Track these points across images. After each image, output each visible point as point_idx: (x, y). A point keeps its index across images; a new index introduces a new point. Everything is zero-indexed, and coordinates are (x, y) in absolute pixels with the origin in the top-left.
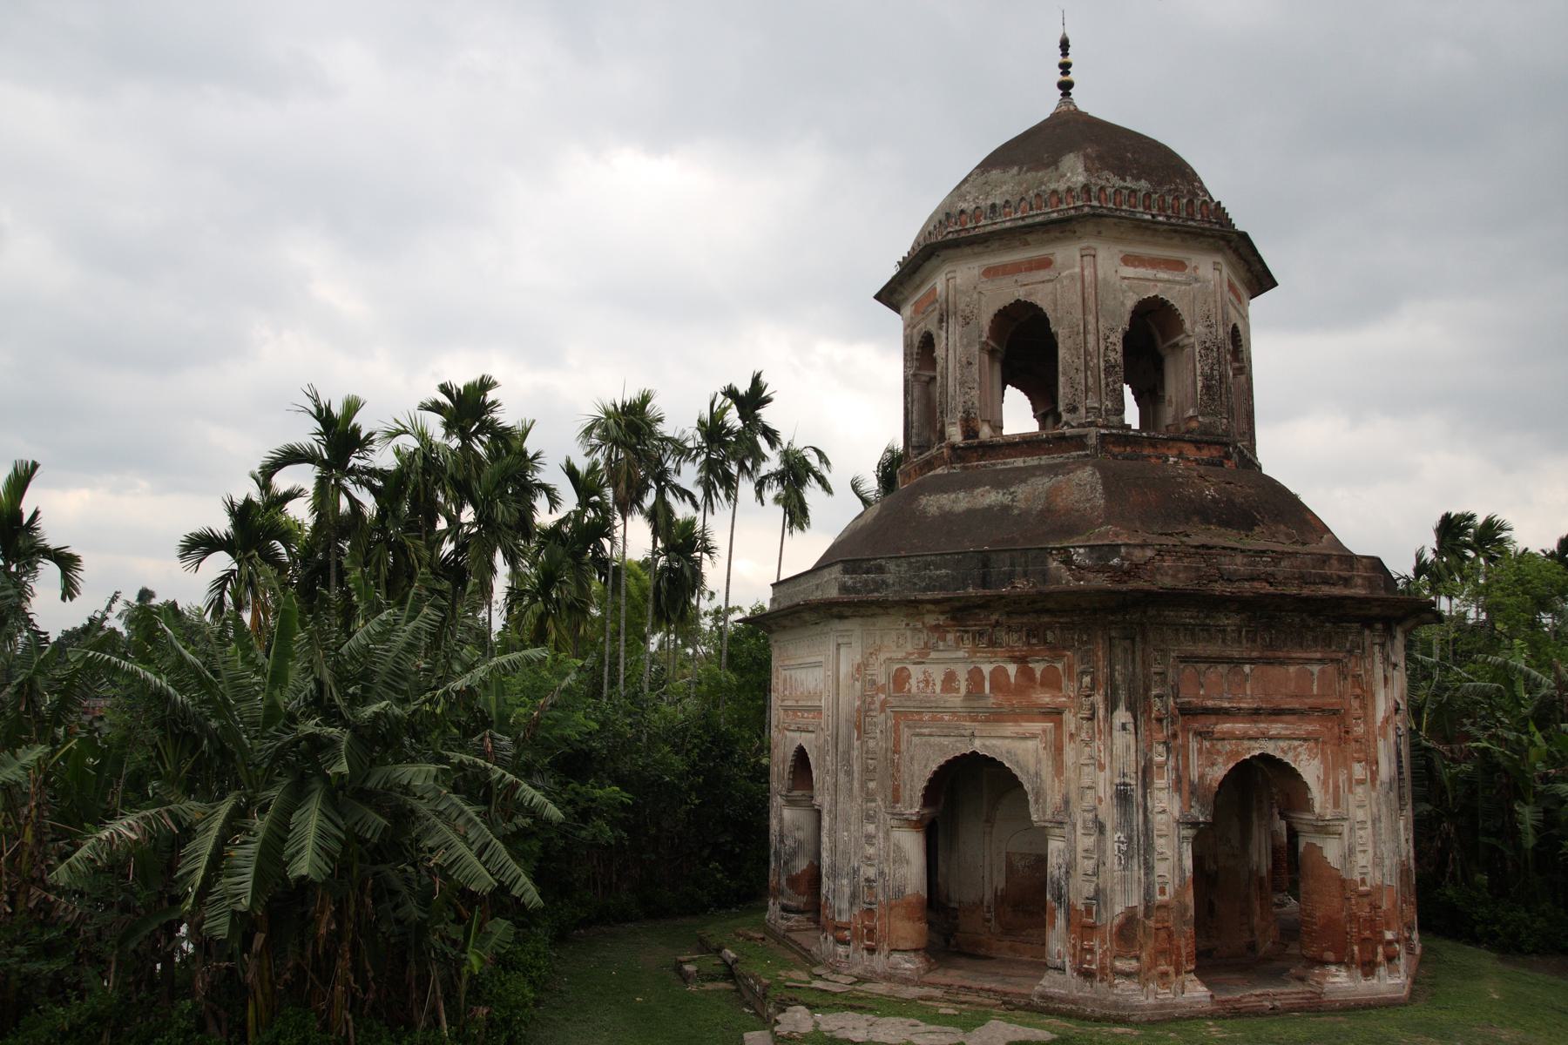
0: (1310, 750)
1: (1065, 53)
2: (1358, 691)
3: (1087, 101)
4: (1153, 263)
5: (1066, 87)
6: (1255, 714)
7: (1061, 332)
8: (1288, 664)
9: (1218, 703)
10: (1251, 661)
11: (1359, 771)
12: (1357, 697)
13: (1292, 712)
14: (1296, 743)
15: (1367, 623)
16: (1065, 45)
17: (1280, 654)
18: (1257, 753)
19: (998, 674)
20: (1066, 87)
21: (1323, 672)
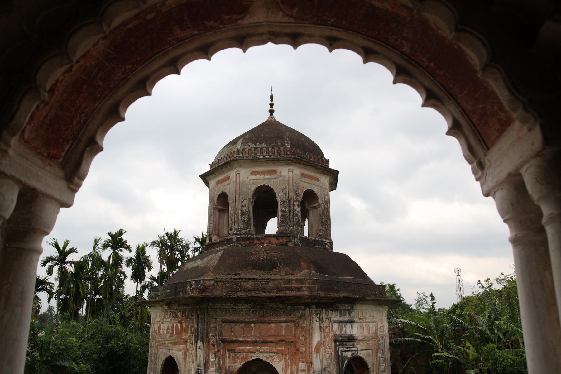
0: (279, 357)
1: (272, 100)
2: (304, 333)
3: (277, 117)
4: (264, 173)
5: (271, 112)
6: (255, 343)
7: (230, 201)
8: (271, 323)
9: (238, 339)
10: (254, 322)
11: (303, 366)
12: (303, 336)
13: (272, 342)
14: (273, 354)
15: (308, 305)
16: (272, 97)
17: (266, 319)
18: (254, 358)
19: (177, 326)
20: (271, 112)
21: (287, 326)
